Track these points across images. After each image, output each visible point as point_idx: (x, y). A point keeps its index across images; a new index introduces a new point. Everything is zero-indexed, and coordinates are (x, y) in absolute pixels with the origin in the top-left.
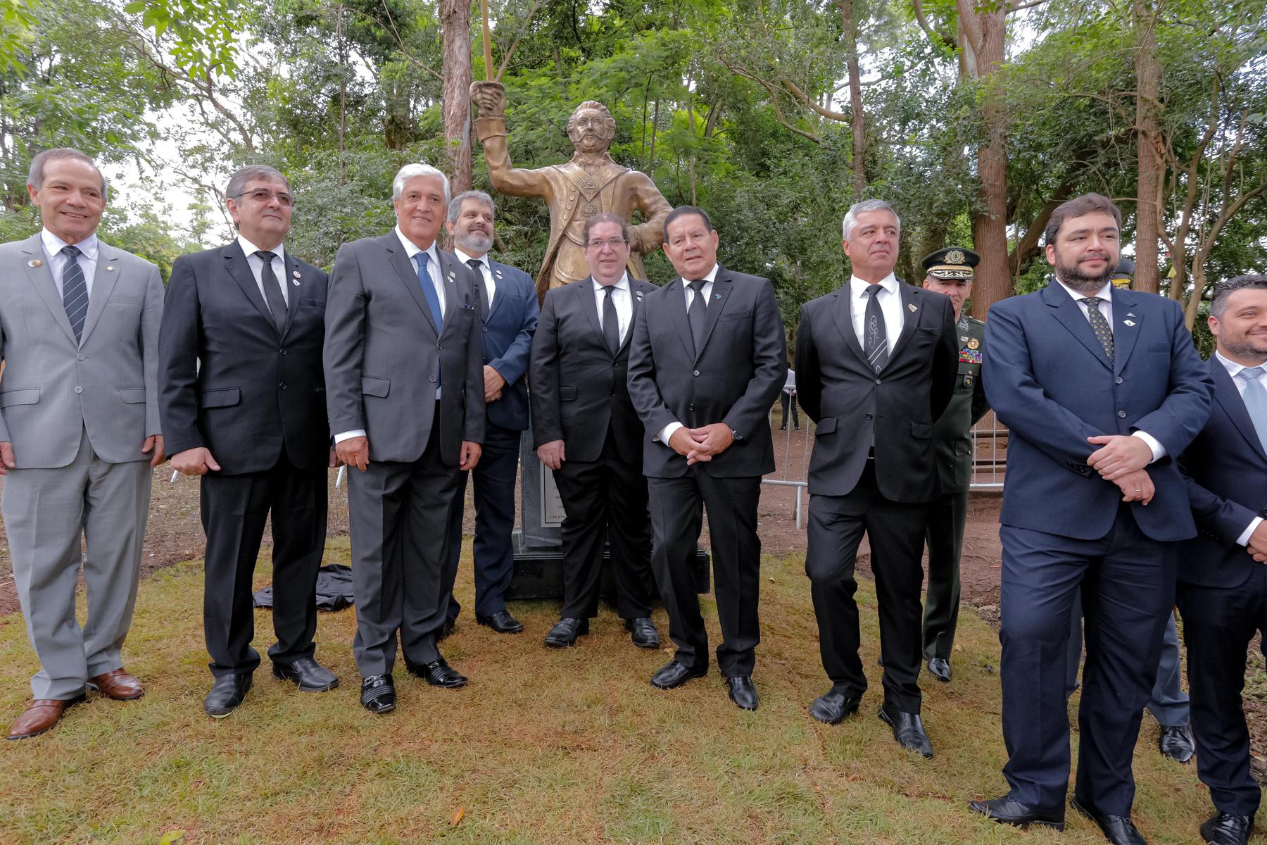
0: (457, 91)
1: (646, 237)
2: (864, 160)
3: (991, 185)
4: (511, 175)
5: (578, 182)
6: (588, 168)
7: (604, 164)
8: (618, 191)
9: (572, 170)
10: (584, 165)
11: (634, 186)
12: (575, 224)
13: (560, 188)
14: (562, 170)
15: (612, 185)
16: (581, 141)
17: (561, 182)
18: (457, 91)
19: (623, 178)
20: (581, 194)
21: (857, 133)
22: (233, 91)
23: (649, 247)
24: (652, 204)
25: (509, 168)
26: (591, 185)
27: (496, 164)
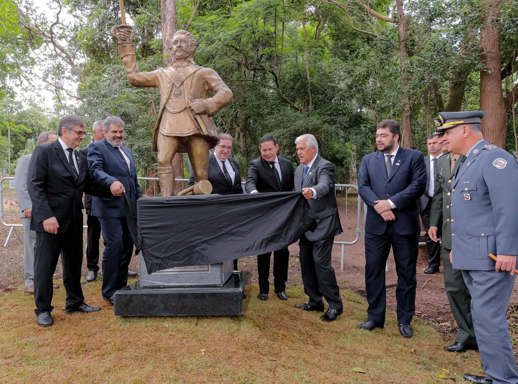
0: (169, 27)
1: (210, 106)
2: (406, 46)
3: (489, 52)
4: (138, 76)
5: (172, 77)
6: (178, 69)
7: (188, 65)
8: (195, 81)
9: (170, 71)
10: (176, 67)
11: (204, 77)
12: (170, 101)
13: (163, 81)
14: (164, 71)
15: (191, 77)
16: (175, 54)
17: (164, 77)
18: (169, 27)
19: (198, 72)
20: (173, 84)
21: (401, 29)
22: (64, 37)
23: (213, 111)
24: (215, 86)
25: (137, 72)
26: (179, 78)
27: (129, 70)
